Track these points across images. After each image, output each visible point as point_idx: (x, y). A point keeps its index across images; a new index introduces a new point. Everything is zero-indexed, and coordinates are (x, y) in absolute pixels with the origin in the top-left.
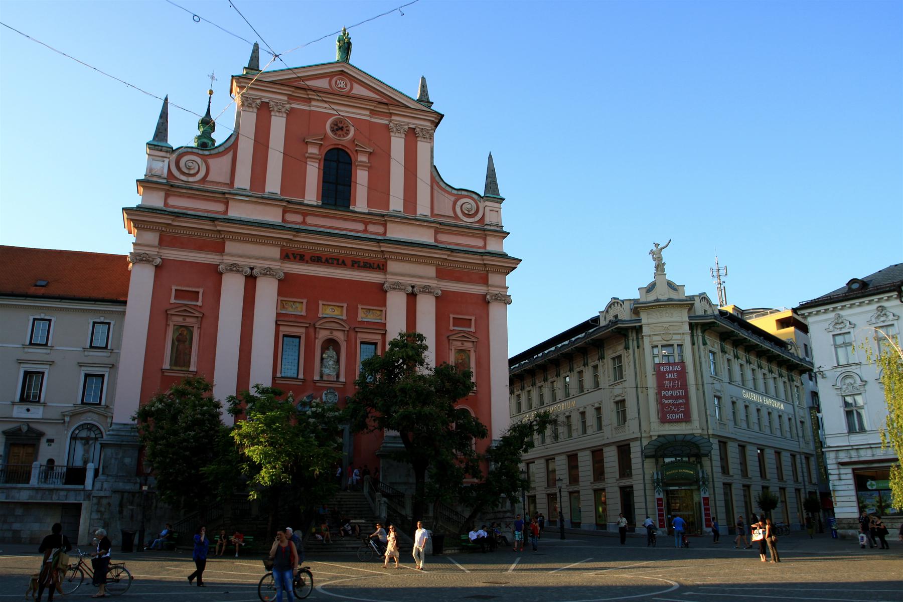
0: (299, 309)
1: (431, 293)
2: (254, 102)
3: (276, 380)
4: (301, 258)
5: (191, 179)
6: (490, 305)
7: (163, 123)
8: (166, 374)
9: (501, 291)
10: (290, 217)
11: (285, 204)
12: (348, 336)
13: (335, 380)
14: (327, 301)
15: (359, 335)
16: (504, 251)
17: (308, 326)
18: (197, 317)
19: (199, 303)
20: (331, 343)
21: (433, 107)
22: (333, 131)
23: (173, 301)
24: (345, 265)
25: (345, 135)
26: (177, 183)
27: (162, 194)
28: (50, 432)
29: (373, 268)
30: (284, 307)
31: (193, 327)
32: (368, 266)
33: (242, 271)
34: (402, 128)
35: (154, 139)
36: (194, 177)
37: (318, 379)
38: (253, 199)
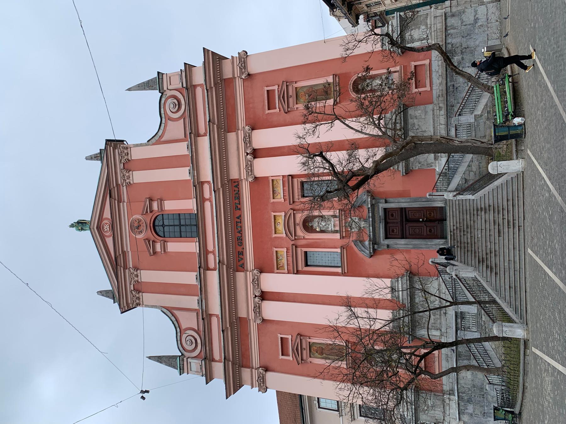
1: (249, 135)
2: (135, 296)
3: (345, 273)
4: (241, 254)
6: (251, 73)
7: (165, 362)
9: (236, 62)
10: (211, 264)
11: (202, 271)
12: (299, 210)
13: (338, 219)
14: (272, 229)
15: (296, 200)
16: (202, 65)
17: (294, 246)
18: (301, 339)
19: (290, 337)
20: (307, 226)
22: (141, 232)
23: (290, 358)
24: (240, 216)
25: (142, 222)
27: (213, 363)
29: (239, 190)
30: (283, 266)
31: (309, 342)
32: (237, 195)
33: (259, 304)
34: (125, 175)
35: (177, 369)
36: (197, 339)
37: (339, 234)
38: (203, 295)
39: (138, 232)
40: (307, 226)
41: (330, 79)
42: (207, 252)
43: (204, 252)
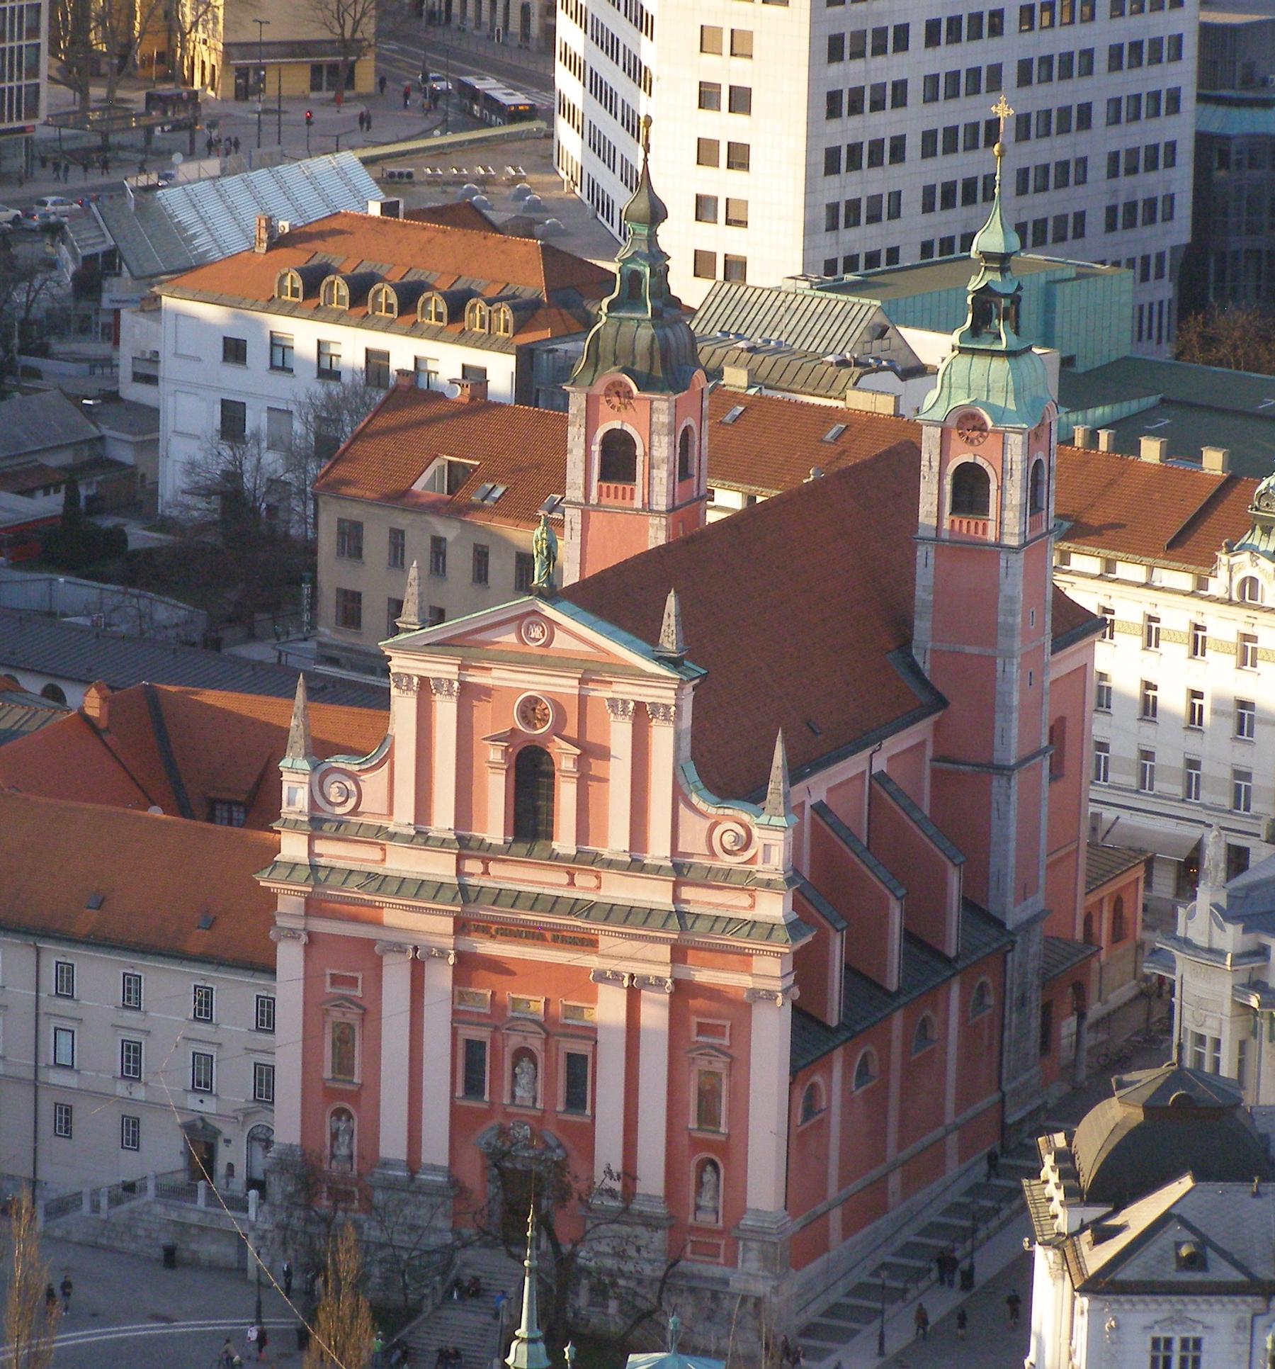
5: (339, 811)
8: (327, 1085)
19: (359, 993)
20: (523, 1054)
23: (328, 989)
26: (325, 816)
28: (227, 1130)
30: (464, 1000)
39: (524, 708)
41: (723, 1129)
43: (487, 854)
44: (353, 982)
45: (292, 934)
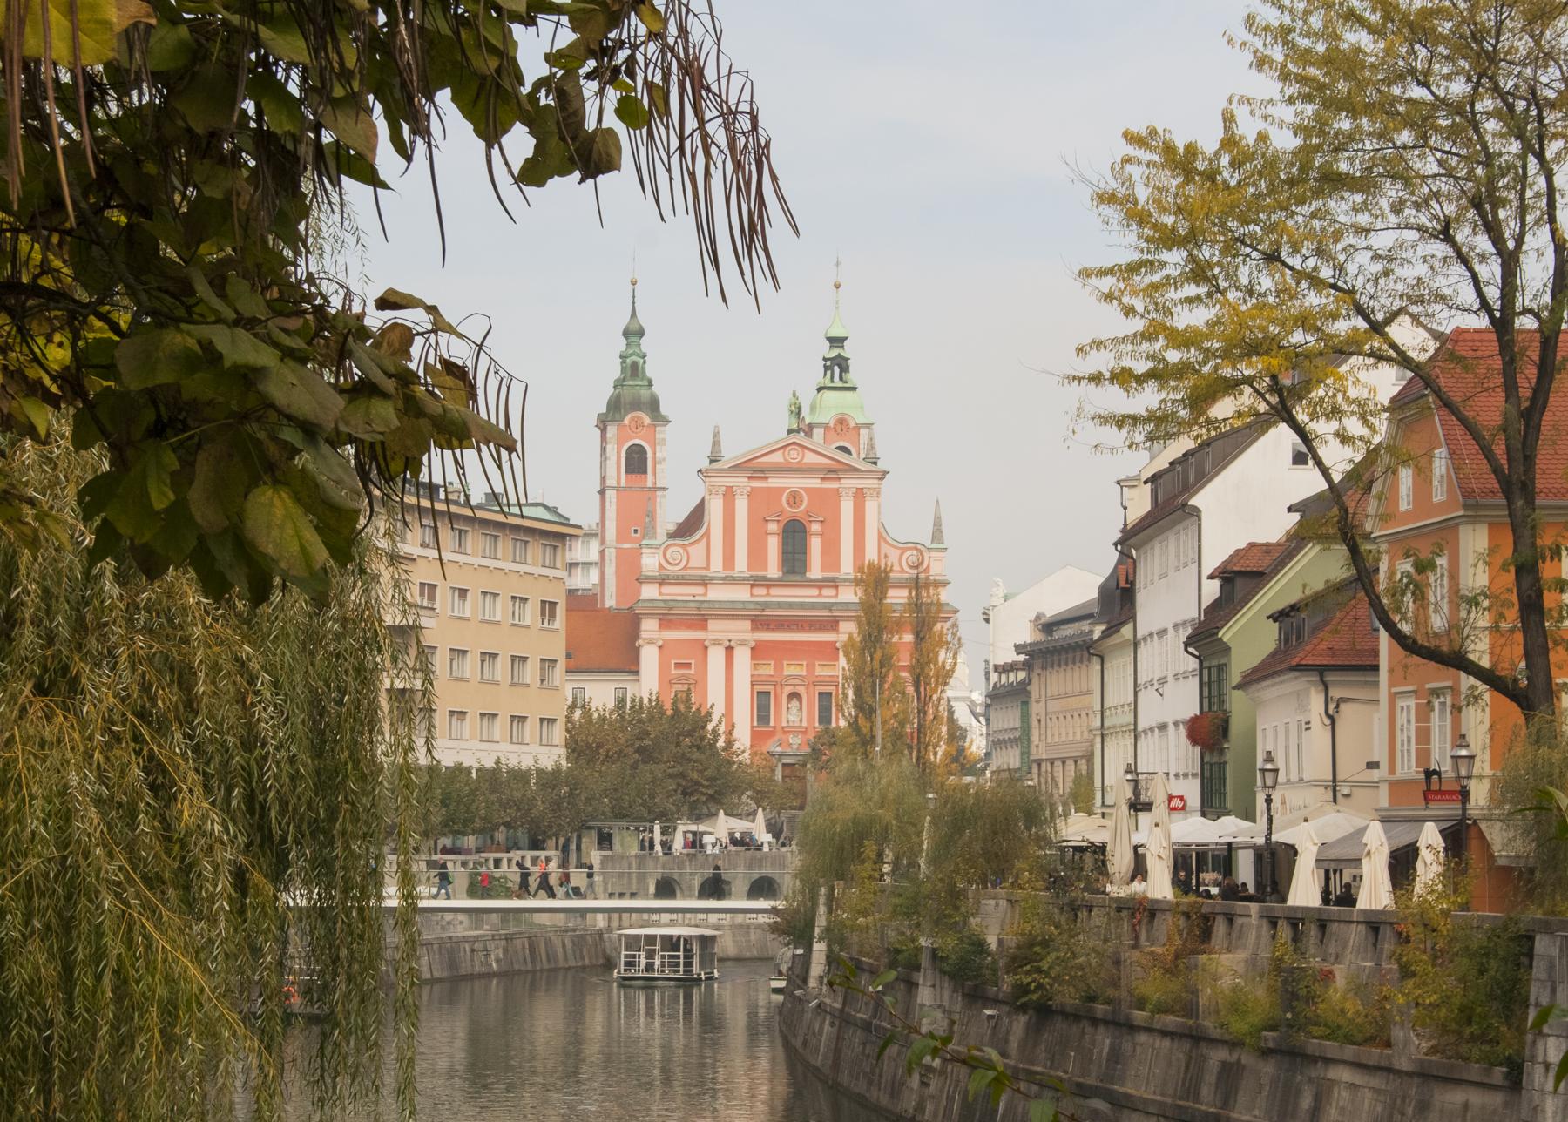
0: (767, 670)
10: (757, 591)
19: (692, 672)
21: (881, 466)
23: (673, 672)
30: (755, 669)
40: (794, 695)
42: (768, 587)
43: (768, 583)
44: (688, 665)
45: (651, 642)
